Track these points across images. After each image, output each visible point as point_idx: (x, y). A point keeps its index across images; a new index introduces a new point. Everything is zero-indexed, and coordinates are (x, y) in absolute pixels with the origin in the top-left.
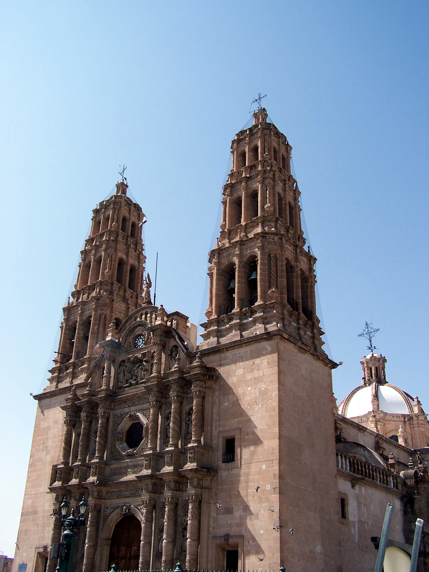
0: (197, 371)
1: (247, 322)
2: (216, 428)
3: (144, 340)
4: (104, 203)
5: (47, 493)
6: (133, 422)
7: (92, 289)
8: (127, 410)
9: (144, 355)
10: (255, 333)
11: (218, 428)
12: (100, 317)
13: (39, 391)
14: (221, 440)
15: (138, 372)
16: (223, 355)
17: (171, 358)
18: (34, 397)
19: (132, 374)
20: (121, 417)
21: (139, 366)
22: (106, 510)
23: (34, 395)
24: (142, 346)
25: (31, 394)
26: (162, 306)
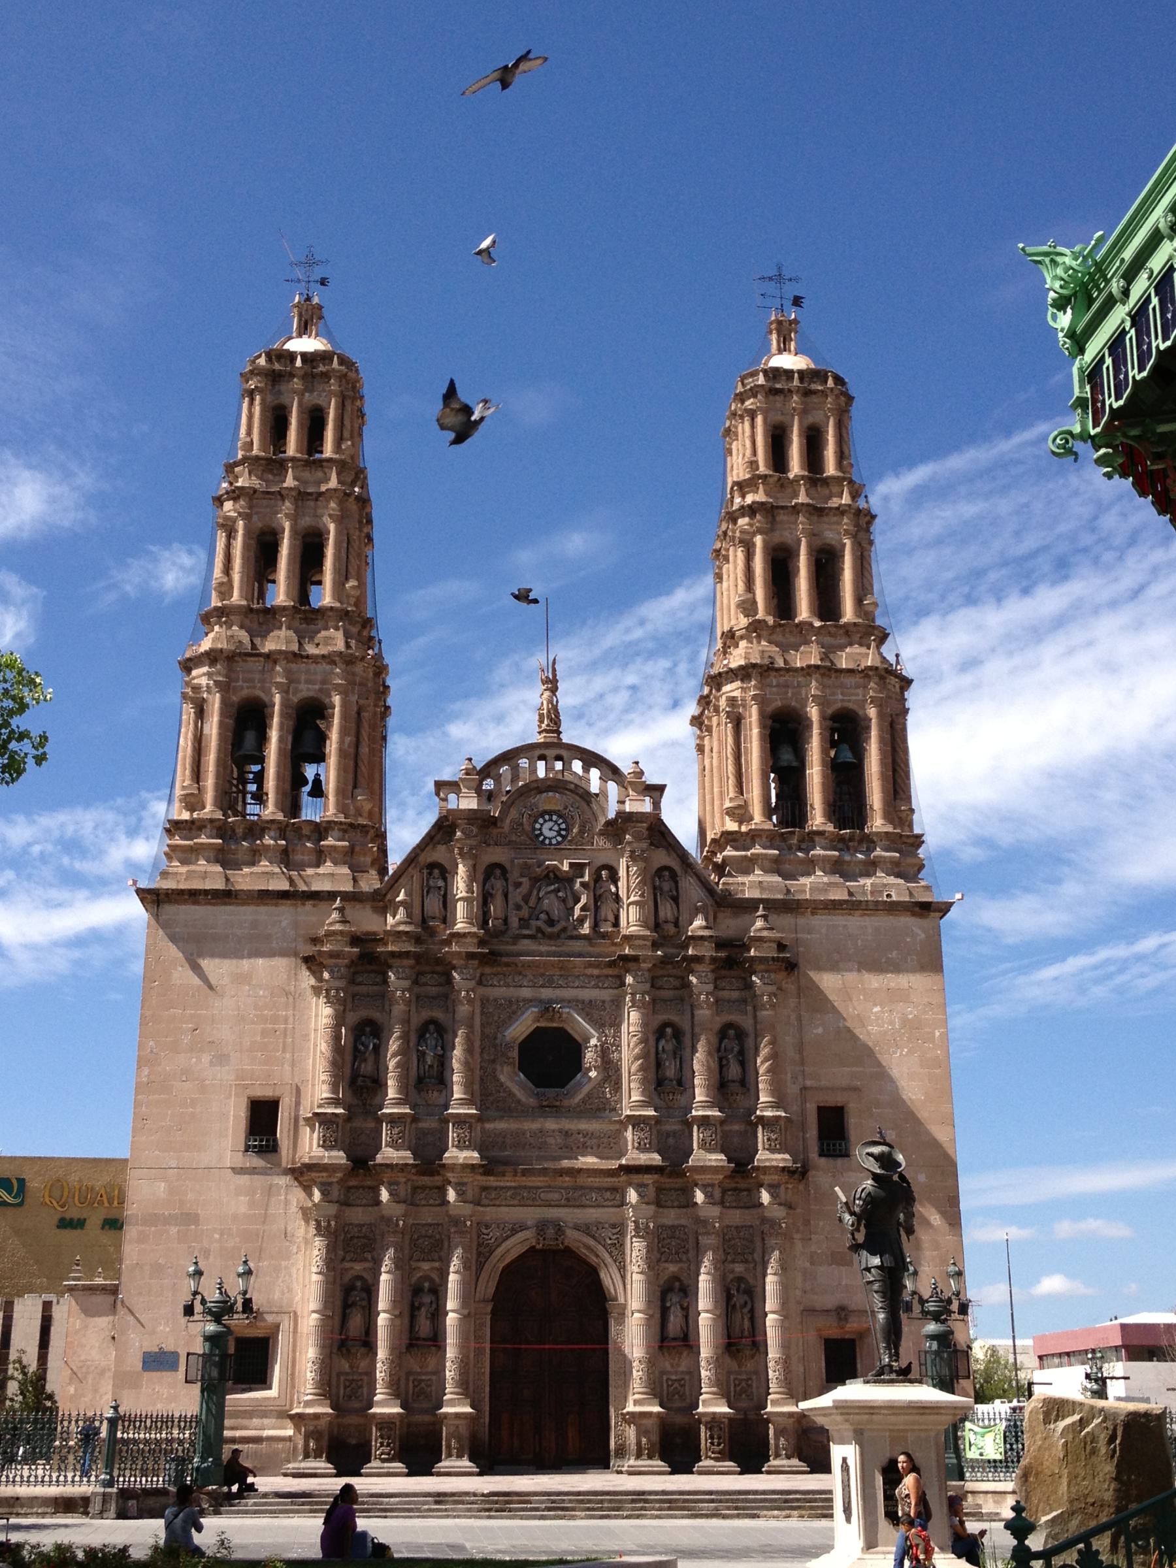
0: (770, 952)
2: (795, 1078)
3: (563, 830)
5: (233, 1169)
6: (543, 1024)
8: (526, 993)
11: (800, 1079)
12: (359, 713)
16: (801, 921)
18: (139, 892)
20: (513, 1008)
22: (485, 1231)
24: (559, 843)
25: (135, 882)
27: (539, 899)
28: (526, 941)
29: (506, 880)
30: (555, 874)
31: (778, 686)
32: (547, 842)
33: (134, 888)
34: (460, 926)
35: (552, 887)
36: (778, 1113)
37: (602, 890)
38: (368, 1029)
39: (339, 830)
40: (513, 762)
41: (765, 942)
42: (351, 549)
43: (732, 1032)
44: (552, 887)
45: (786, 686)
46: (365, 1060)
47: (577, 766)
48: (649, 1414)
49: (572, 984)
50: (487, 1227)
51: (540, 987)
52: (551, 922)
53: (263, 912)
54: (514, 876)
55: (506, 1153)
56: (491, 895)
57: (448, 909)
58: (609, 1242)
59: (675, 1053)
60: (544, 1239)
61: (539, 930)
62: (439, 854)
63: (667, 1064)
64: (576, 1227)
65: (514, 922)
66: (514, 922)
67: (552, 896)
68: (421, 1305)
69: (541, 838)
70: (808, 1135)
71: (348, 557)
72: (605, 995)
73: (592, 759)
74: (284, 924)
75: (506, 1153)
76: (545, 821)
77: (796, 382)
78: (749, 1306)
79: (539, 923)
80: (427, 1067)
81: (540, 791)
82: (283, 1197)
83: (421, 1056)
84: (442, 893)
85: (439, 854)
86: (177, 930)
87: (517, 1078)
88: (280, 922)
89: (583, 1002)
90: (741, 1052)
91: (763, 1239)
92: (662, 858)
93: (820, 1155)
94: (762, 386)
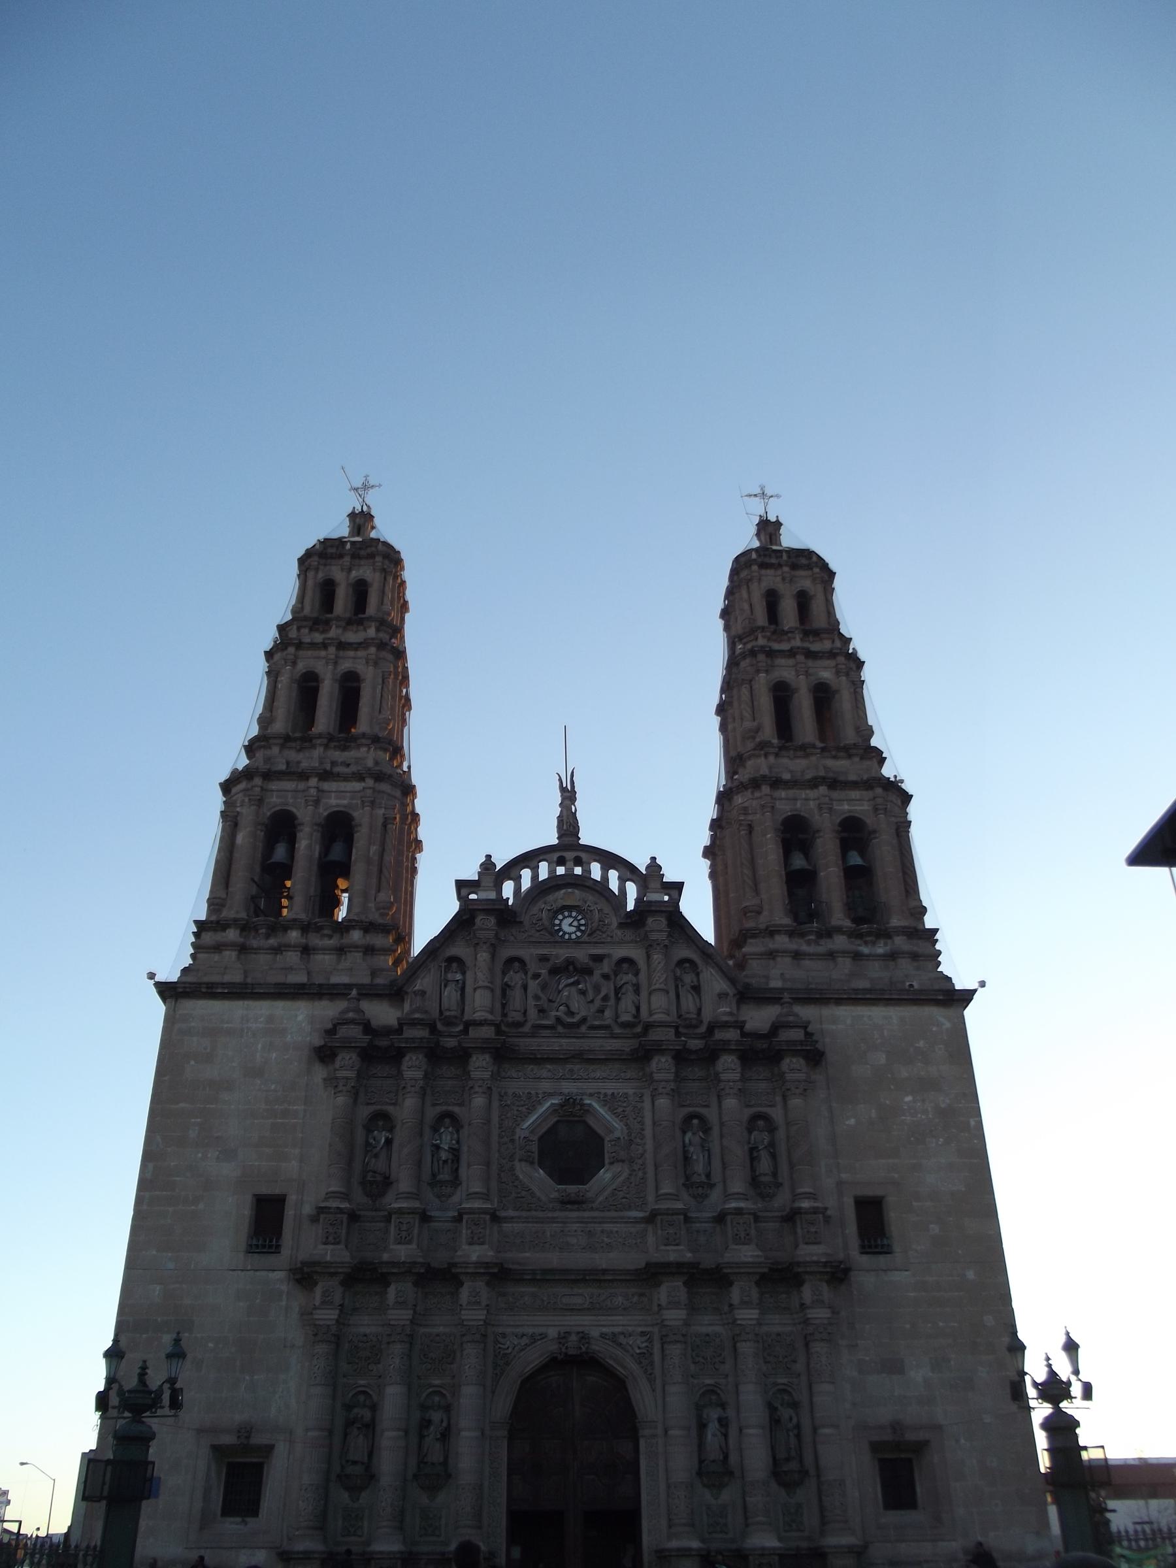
1: (867, 956)
4: (348, 546)
7: (335, 746)
8: (546, 1086)
9: (598, 959)
10: (908, 984)
12: (385, 825)
13: (170, 973)
14: (849, 1202)
15: (568, 997)
16: (828, 1011)
17: (682, 986)
19: (551, 998)
20: (532, 1102)
21: (577, 983)
22: (501, 1340)
23: (157, 979)
24: (578, 937)
26: (653, 859)
27: (560, 992)
28: (546, 1032)
29: (526, 973)
30: (575, 969)
31: (787, 799)
32: (567, 937)
33: (152, 982)
34: (478, 1016)
35: (572, 980)
36: (816, 1205)
37: (622, 982)
38: (381, 1123)
39: (360, 929)
40: (533, 864)
41: (792, 1027)
42: (386, 690)
43: (761, 1123)
44: (572, 980)
45: (795, 799)
46: (376, 1156)
47: (596, 871)
48: (690, 1549)
49: (592, 1075)
50: (504, 1335)
51: (560, 1079)
52: (571, 1013)
53: (279, 1008)
54: (533, 967)
55: (527, 1255)
56: (509, 986)
57: (467, 1003)
58: (638, 1351)
59: (703, 1147)
60: (567, 1348)
61: (558, 1019)
62: (458, 949)
63: (695, 1157)
64: (603, 1335)
65: (532, 1013)
66: (532, 1013)
67: (573, 989)
68: (429, 1422)
69: (561, 933)
70: (847, 1231)
71: (382, 696)
72: (629, 1089)
73: (610, 860)
74: (300, 1018)
75: (527, 1255)
76: (565, 917)
77: (785, 556)
78: (795, 1421)
79: (558, 1014)
80: (441, 1162)
81: (558, 887)
82: (284, 1303)
83: (438, 1147)
84: (460, 985)
85: (458, 949)
86: (193, 1024)
87: (536, 1174)
88: (296, 1016)
89: (606, 1095)
90: (772, 1144)
91: (807, 1345)
92: (683, 952)
93: (862, 1253)
94: (755, 560)
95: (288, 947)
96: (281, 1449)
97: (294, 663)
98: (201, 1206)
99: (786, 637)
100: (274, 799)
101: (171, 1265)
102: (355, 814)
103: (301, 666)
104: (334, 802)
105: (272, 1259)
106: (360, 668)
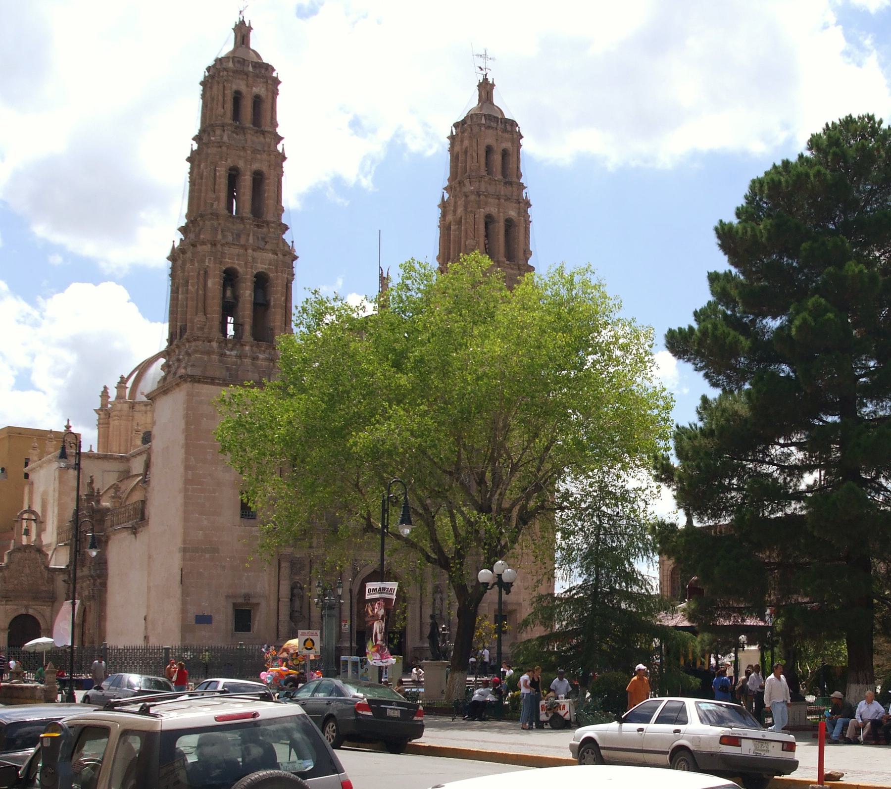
95: (246, 357)
96: (263, 604)
97: (226, 160)
98: (217, 494)
99: (494, 183)
100: (227, 260)
101: (205, 522)
102: (271, 275)
103: (230, 163)
104: (261, 267)
105: (252, 521)
106: (265, 169)
